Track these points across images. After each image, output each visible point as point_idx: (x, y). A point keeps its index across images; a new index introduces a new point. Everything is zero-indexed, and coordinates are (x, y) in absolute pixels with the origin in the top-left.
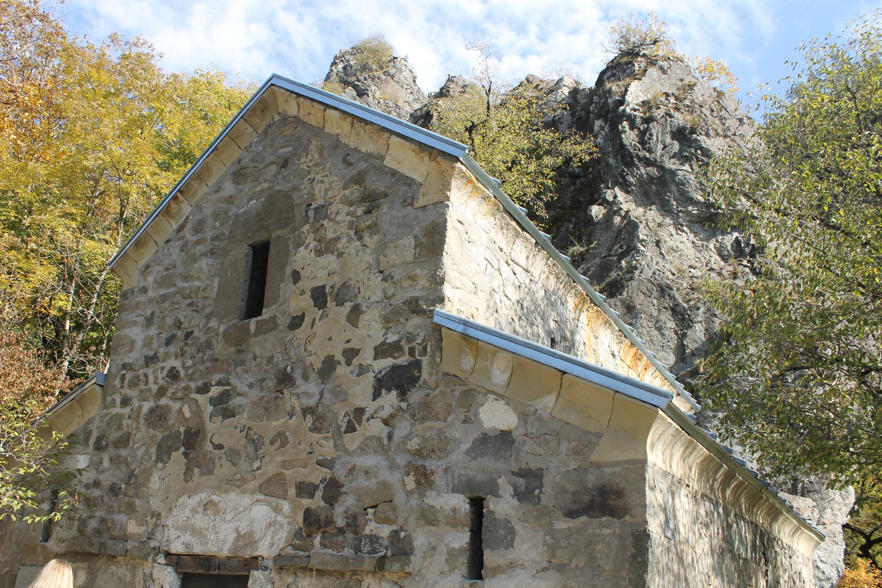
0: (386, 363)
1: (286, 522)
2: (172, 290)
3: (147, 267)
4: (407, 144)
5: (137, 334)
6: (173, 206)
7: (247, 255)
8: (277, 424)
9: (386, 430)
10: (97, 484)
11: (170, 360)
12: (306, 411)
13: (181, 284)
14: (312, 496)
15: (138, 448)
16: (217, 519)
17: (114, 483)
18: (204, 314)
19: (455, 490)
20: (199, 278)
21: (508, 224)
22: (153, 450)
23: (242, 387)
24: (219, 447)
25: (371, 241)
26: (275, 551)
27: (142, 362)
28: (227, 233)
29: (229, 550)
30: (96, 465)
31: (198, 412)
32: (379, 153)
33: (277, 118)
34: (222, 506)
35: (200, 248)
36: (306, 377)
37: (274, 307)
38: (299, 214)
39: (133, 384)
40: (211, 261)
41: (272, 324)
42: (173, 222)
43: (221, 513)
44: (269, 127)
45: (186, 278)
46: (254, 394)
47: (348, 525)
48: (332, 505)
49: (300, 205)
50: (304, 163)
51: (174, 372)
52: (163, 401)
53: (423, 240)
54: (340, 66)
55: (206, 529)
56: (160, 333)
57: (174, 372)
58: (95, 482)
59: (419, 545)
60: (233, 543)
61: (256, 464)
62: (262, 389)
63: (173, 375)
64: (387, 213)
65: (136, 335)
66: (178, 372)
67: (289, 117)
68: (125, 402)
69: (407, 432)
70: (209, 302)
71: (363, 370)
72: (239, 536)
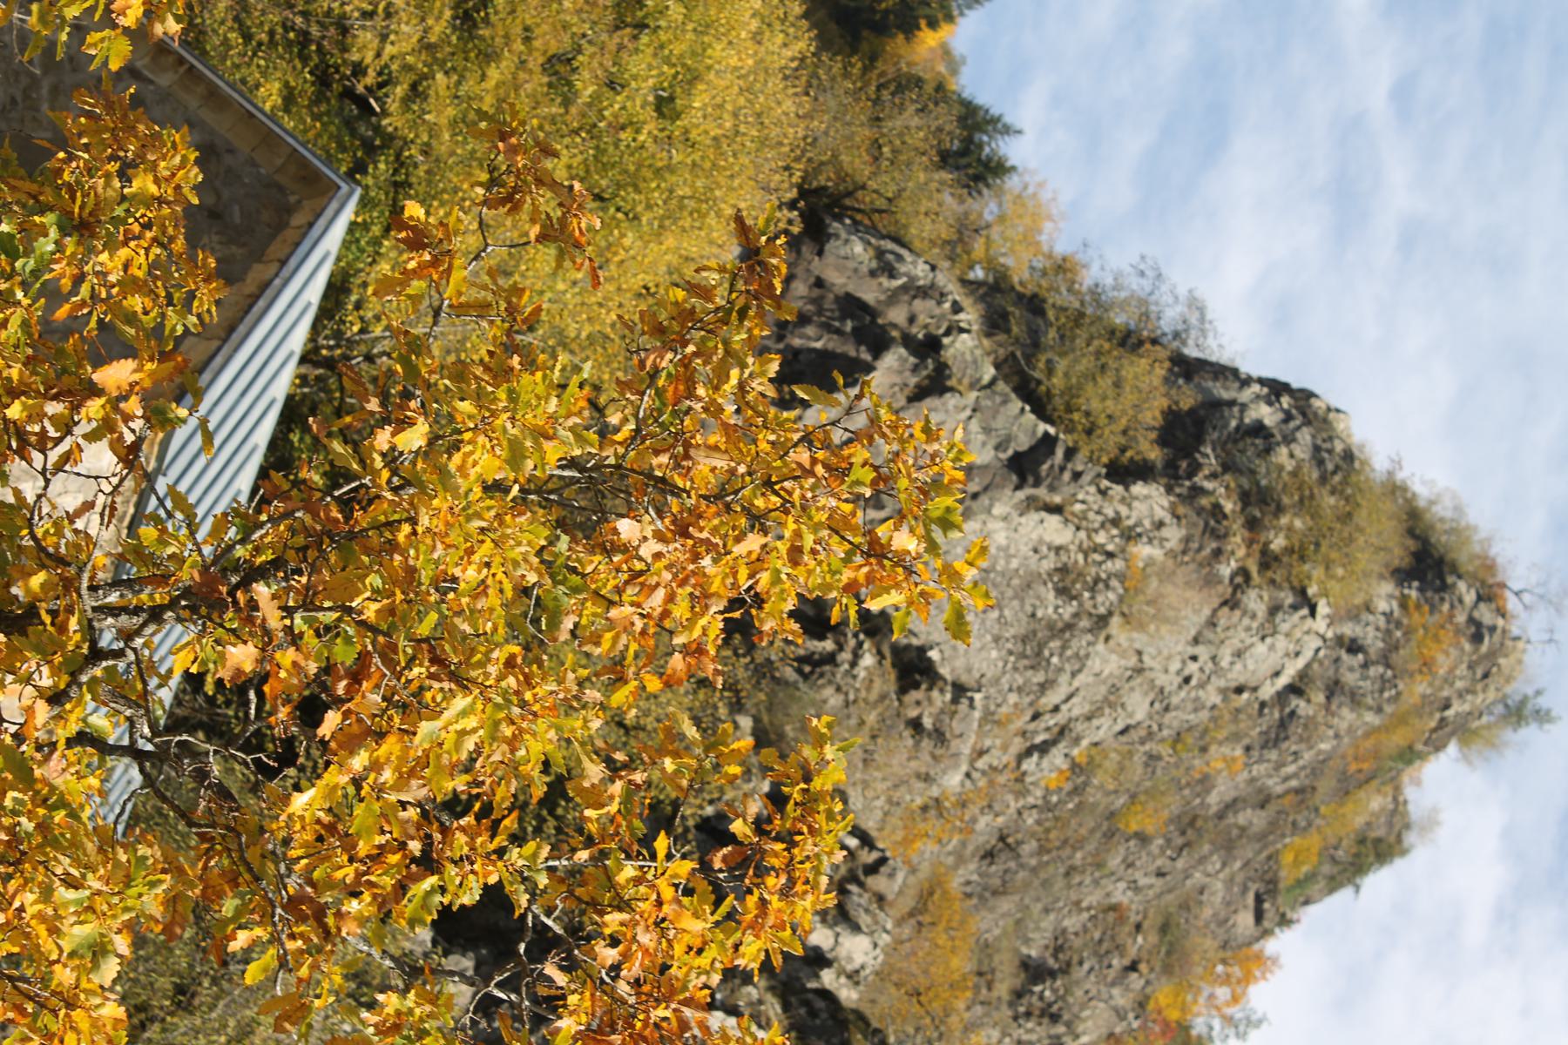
4: (204, 357)
6: (171, 59)
21: (128, 502)
33: (293, 199)
42: (146, 60)
44: (281, 189)
54: (1267, 415)
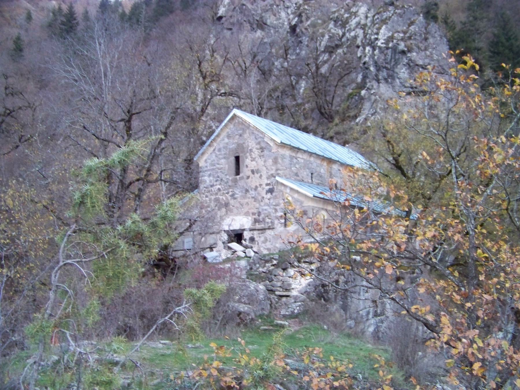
0: (268, 187)
5: (206, 178)
8: (246, 200)
12: (253, 198)
13: (218, 166)
23: (237, 192)
25: (263, 159)
30: (200, 212)
31: (227, 198)
35: (221, 156)
38: (246, 150)
39: (209, 192)
41: (242, 178)
45: (218, 164)
46: (240, 194)
50: (246, 136)
63: (219, 190)
64: (266, 152)
71: (263, 189)
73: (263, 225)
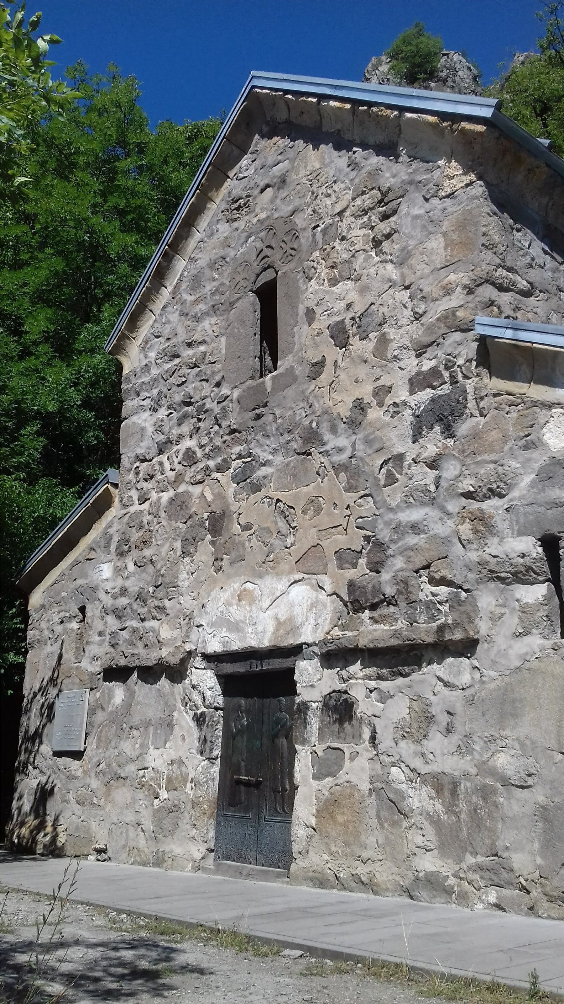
1: (329, 601)
2: (177, 361)
3: (146, 342)
7: (253, 304)
8: (308, 490)
9: (432, 474)
10: (124, 591)
11: (184, 442)
12: (338, 468)
14: (355, 566)
15: (162, 545)
16: (254, 608)
17: (142, 588)
18: (214, 382)
19: (521, 533)
20: (203, 342)
22: (178, 544)
23: (265, 456)
24: (247, 527)
26: (320, 636)
27: (154, 451)
28: (228, 283)
29: (270, 641)
30: (118, 571)
31: (220, 496)
32: (390, 141)
34: (257, 592)
36: (334, 430)
37: (290, 357)
38: (305, 239)
40: (214, 320)
43: (257, 602)
46: (279, 459)
47: (399, 592)
48: (378, 572)
49: (305, 229)
51: (190, 454)
52: (182, 488)
53: (454, 237)
55: (243, 622)
56: (171, 413)
57: (190, 454)
58: (121, 589)
59: (485, 606)
60: (274, 633)
61: (290, 540)
62: (286, 455)
65: (145, 420)
66: (194, 452)
67: (279, 123)
68: (143, 500)
69: (457, 472)
70: (218, 366)
72: (279, 624)
73: (401, 624)
